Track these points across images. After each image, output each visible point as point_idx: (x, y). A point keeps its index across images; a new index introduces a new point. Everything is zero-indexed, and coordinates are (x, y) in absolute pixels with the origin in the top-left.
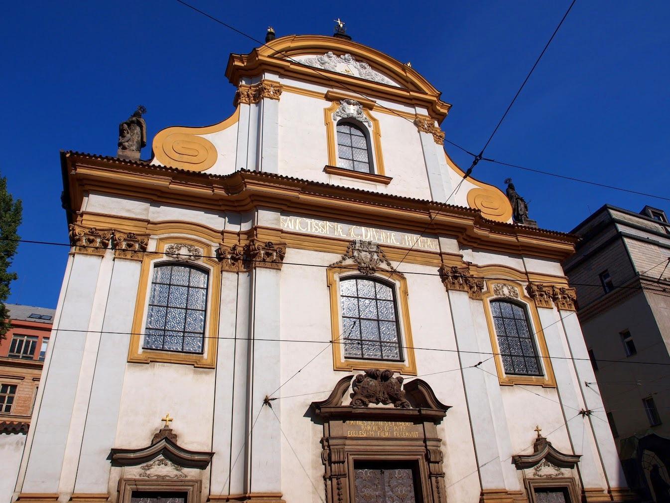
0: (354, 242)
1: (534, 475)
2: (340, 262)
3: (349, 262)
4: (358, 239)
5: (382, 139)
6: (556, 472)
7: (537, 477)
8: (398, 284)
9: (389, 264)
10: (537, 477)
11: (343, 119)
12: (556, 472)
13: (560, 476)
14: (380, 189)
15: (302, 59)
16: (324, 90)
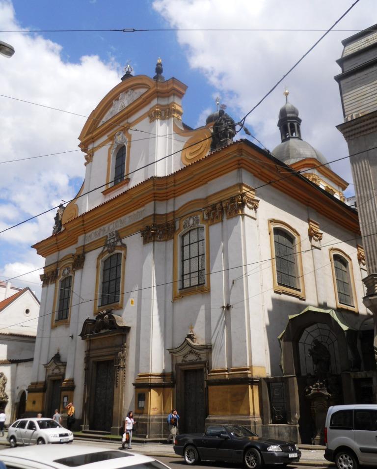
0: (107, 236)
1: (182, 361)
2: (103, 250)
3: (106, 249)
4: (107, 234)
5: (131, 149)
6: (197, 358)
7: (184, 362)
8: (123, 252)
9: (121, 241)
10: (184, 362)
11: (117, 148)
12: (197, 358)
13: (199, 360)
14: (125, 189)
15: (104, 120)
16: (105, 138)
